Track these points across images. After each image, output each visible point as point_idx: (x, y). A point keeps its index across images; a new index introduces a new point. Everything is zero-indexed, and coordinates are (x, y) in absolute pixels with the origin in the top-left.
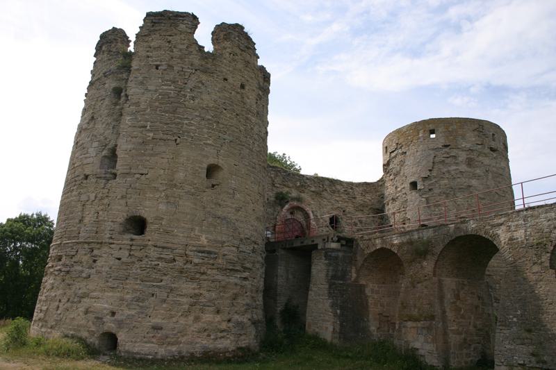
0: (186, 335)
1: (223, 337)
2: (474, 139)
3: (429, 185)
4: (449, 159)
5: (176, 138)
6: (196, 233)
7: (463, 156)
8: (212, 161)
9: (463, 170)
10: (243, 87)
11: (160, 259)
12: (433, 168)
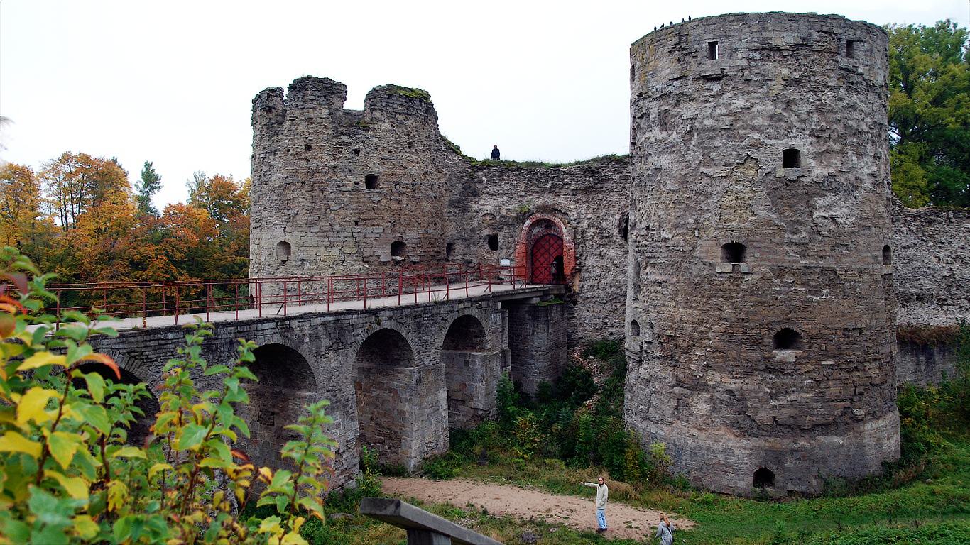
9: (653, 140)
10: (308, 148)
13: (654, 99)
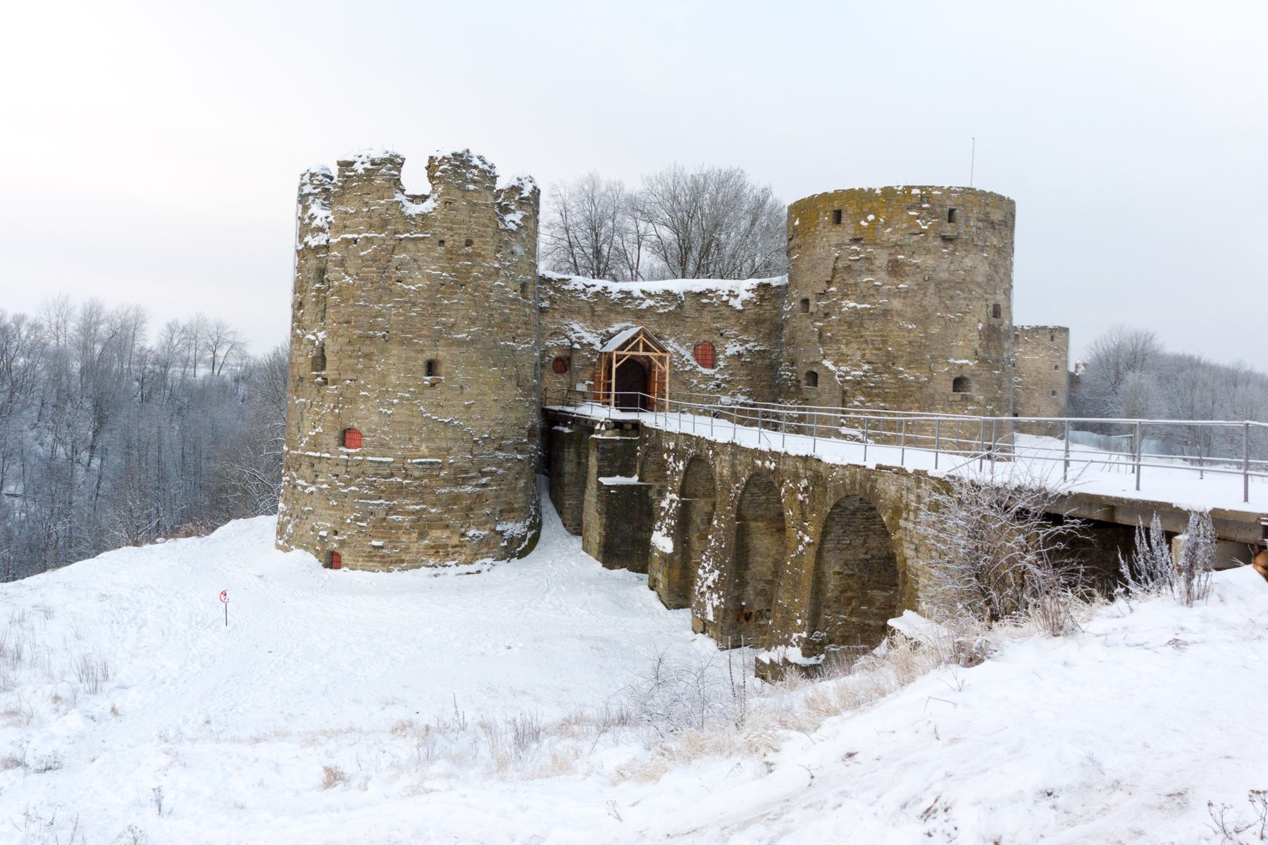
0: (410, 553)
1: (456, 552)
2: (905, 226)
3: (826, 306)
4: (859, 264)
5: (384, 333)
6: (415, 443)
7: (882, 259)
8: (429, 355)
11: (375, 475)
12: (833, 277)
13: (883, 247)
